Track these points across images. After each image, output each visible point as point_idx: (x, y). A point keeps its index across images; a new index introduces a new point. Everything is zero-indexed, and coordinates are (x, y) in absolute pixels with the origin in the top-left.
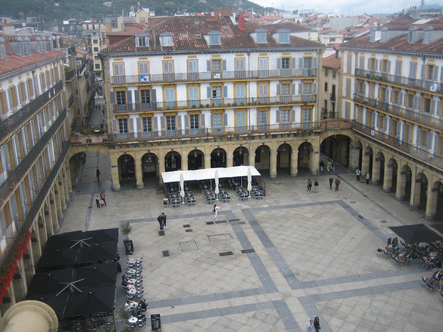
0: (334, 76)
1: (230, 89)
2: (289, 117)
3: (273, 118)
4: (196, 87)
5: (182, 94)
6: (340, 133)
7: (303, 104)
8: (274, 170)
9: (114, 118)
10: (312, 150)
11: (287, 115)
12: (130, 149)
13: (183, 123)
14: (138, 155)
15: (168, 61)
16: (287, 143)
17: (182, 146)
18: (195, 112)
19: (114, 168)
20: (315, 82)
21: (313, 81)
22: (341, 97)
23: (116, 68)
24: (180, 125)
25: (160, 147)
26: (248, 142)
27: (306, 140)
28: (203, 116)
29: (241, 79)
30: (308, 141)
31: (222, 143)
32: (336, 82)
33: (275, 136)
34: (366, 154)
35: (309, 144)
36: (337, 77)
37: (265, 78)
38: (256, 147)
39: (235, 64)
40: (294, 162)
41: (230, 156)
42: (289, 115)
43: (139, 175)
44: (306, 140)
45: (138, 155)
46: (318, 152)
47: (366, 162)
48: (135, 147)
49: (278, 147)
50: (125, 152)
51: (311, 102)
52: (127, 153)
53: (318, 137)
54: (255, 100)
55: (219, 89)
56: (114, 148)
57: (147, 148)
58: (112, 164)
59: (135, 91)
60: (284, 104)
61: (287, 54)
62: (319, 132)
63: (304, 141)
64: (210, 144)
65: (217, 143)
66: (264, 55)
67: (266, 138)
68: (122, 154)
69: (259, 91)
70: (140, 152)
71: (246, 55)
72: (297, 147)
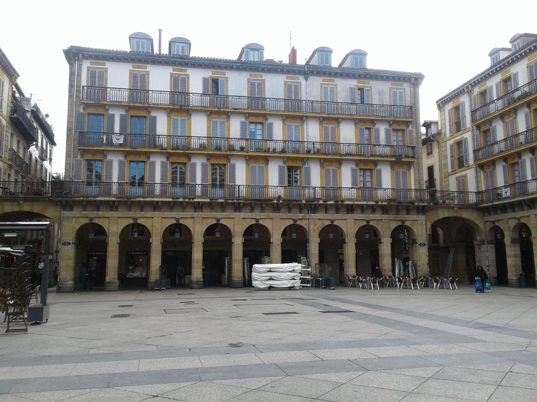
1: (278, 130)
2: (371, 182)
3: (346, 176)
4: (223, 119)
5: (199, 127)
6: (458, 215)
7: (394, 159)
8: (351, 269)
9: (79, 157)
10: (414, 242)
11: (368, 179)
12: (100, 213)
13: (199, 172)
14: (114, 225)
15: (180, 75)
16: (372, 223)
17: (196, 214)
18: (219, 157)
19: (66, 247)
20: (410, 127)
21: (408, 126)
22: (445, 177)
23: (92, 75)
24: (194, 177)
25: (157, 214)
26: (307, 216)
27: (403, 222)
28: (233, 167)
29: (294, 114)
30: (407, 224)
31: (263, 215)
33: (350, 209)
34: (513, 241)
35: (409, 230)
36: (436, 151)
37: (334, 114)
38: (320, 225)
39: (285, 91)
40: (385, 259)
41: (276, 239)
42: (372, 179)
43: (113, 263)
44: (403, 222)
45: (114, 225)
46: (425, 245)
47: (515, 256)
48: (111, 210)
49: (357, 229)
50: (91, 219)
51: (407, 157)
52: (96, 221)
53: (422, 218)
54: (318, 146)
55: (259, 127)
56: (71, 209)
57: (133, 214)
58: (65, 239)
59: (121, 116)
60: (364, 156)
61: (365, 83)
62: (424, 207)
63: (400, 223)
64: (242, 215)
65: (254, 214)
66: (330, 80)
67: (337, 213)
68: (84, 221)
69: (324, 132)
70: (120, 220)
71: (301, 79)
72: (389, 233)
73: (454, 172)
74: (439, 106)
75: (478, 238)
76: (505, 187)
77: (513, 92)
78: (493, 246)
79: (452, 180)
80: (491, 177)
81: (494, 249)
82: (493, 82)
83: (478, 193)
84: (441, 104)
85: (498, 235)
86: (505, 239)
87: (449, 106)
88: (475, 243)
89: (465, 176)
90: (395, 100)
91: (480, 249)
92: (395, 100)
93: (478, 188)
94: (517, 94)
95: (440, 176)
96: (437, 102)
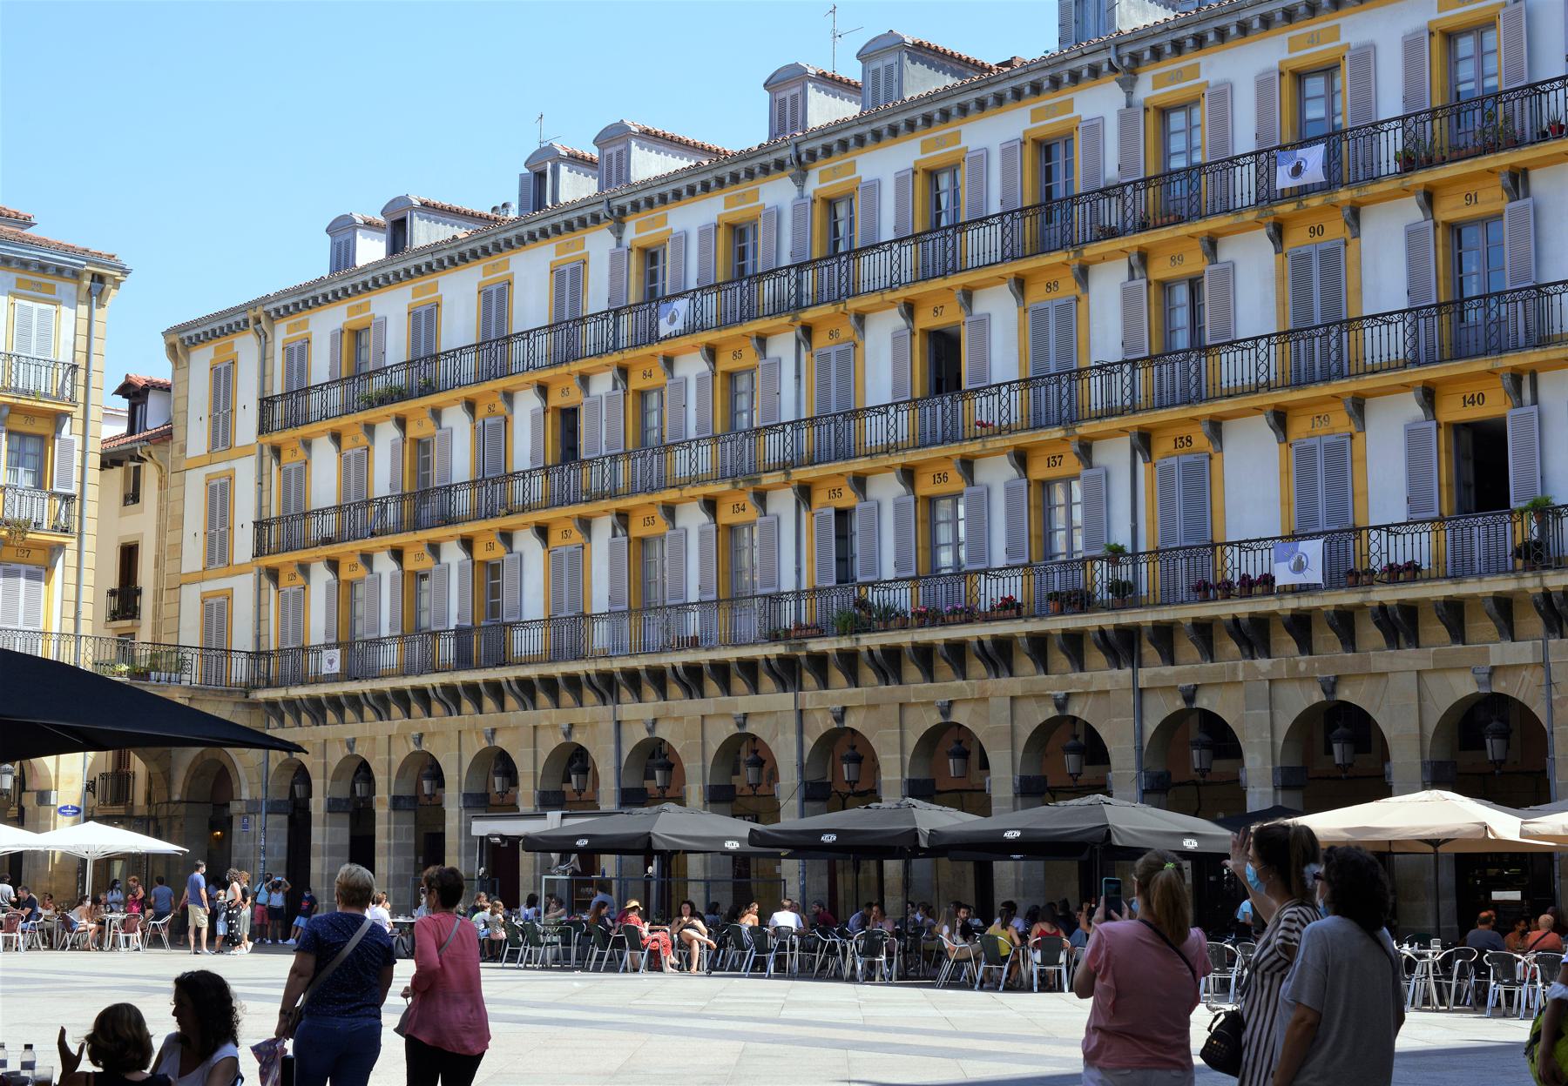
0: (133, 497)
22: (173, 585)
32: (142, 524)
34: (333, 806)
46: (79, 810)
73: (197, 578)
74: (172, 350)
75: (246, 795)
76: (328, 646)
77: (370, 375)
78: (284, 818)
79: (191, 597)
80: (296, 607)
81: (285, 830)
82: (325, 325)
83: (257, 655)
84: (182, 342)
85: (358, 786)
86: (313, 801)
87: (202, 359)
88: (235, 807)
89: (228, 595)
90: (25, 333)
91: (245, 827)
92: (25, 333)
93: (258, 638)
94: (378, 384)
95: (156, 583)
96: (165, 334)
